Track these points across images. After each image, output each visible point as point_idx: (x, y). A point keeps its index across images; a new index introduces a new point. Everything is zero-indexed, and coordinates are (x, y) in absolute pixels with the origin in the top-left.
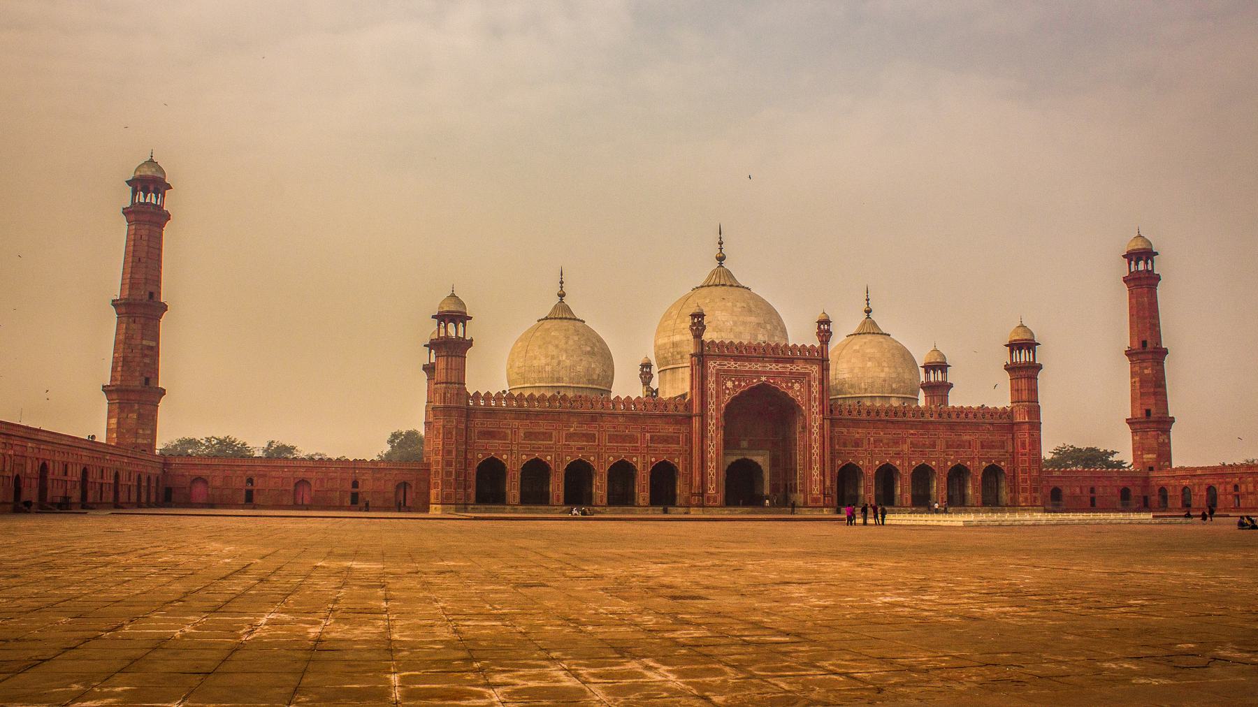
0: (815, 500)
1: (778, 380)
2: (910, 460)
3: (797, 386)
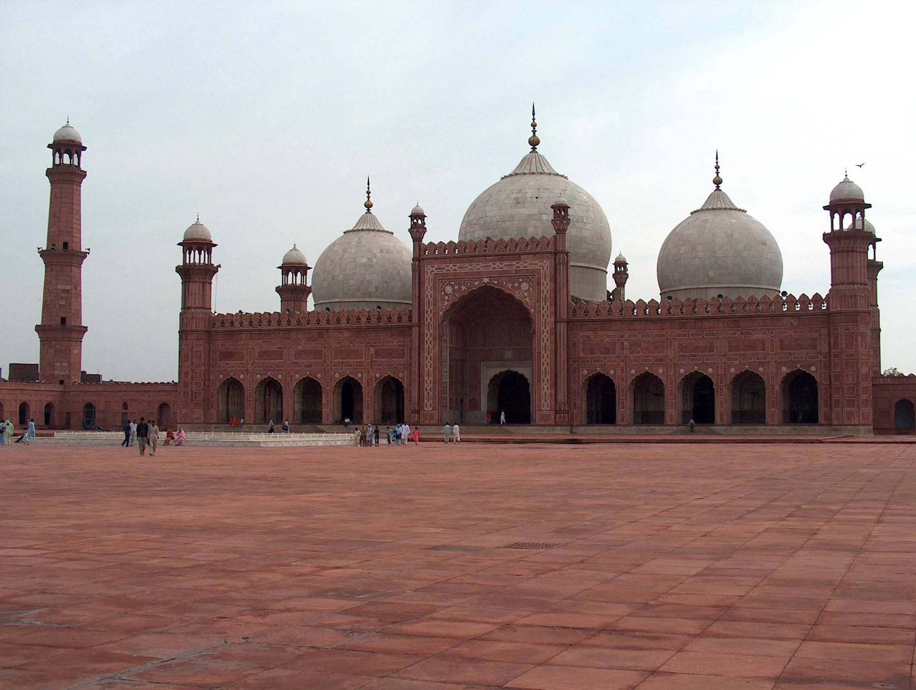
3: (525, 286)
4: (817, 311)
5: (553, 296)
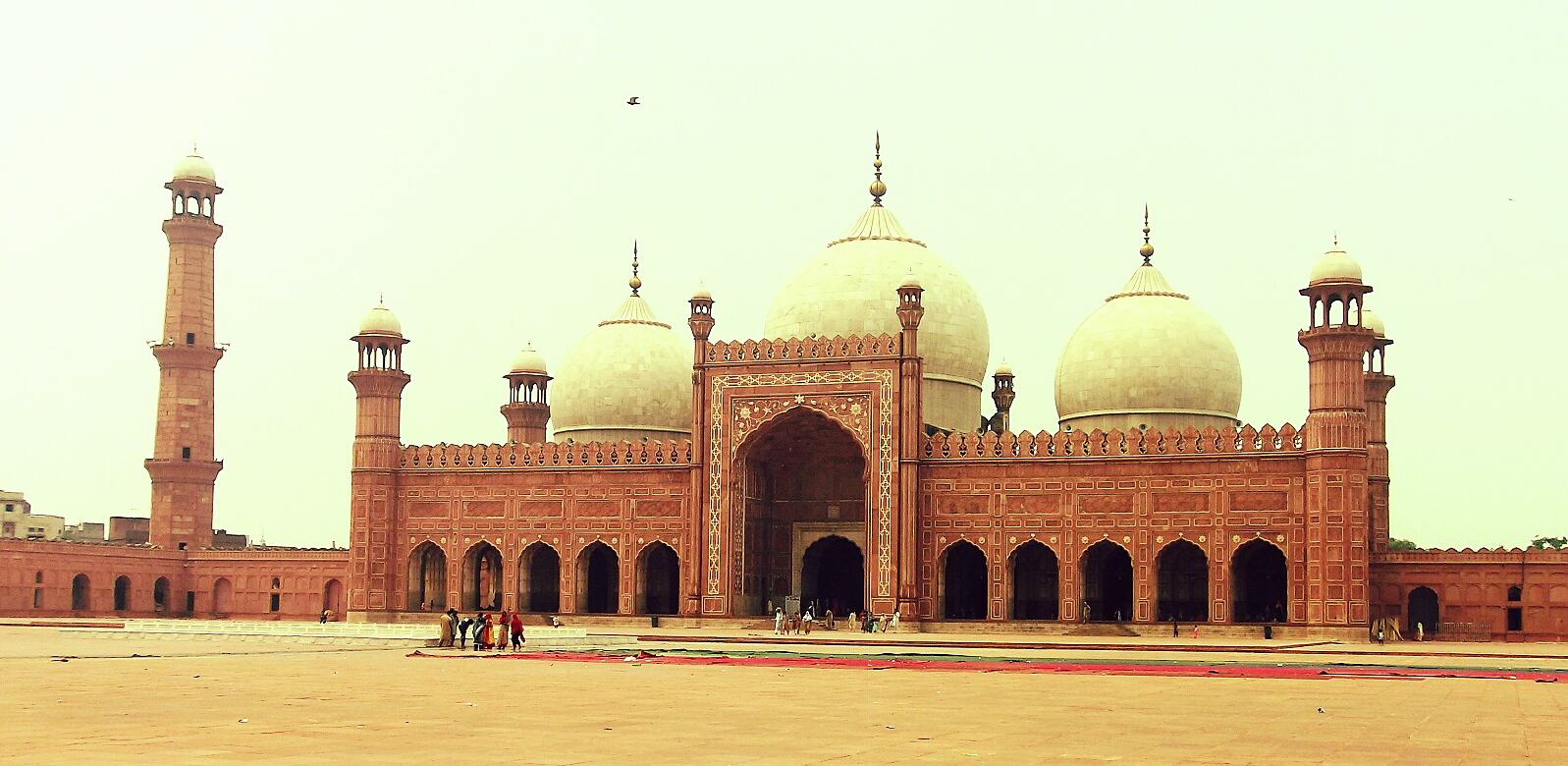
0: (883, 608)
1: (824, 398)
2: (1079, 533)
3: (856, 408)
4: (1287, 451)
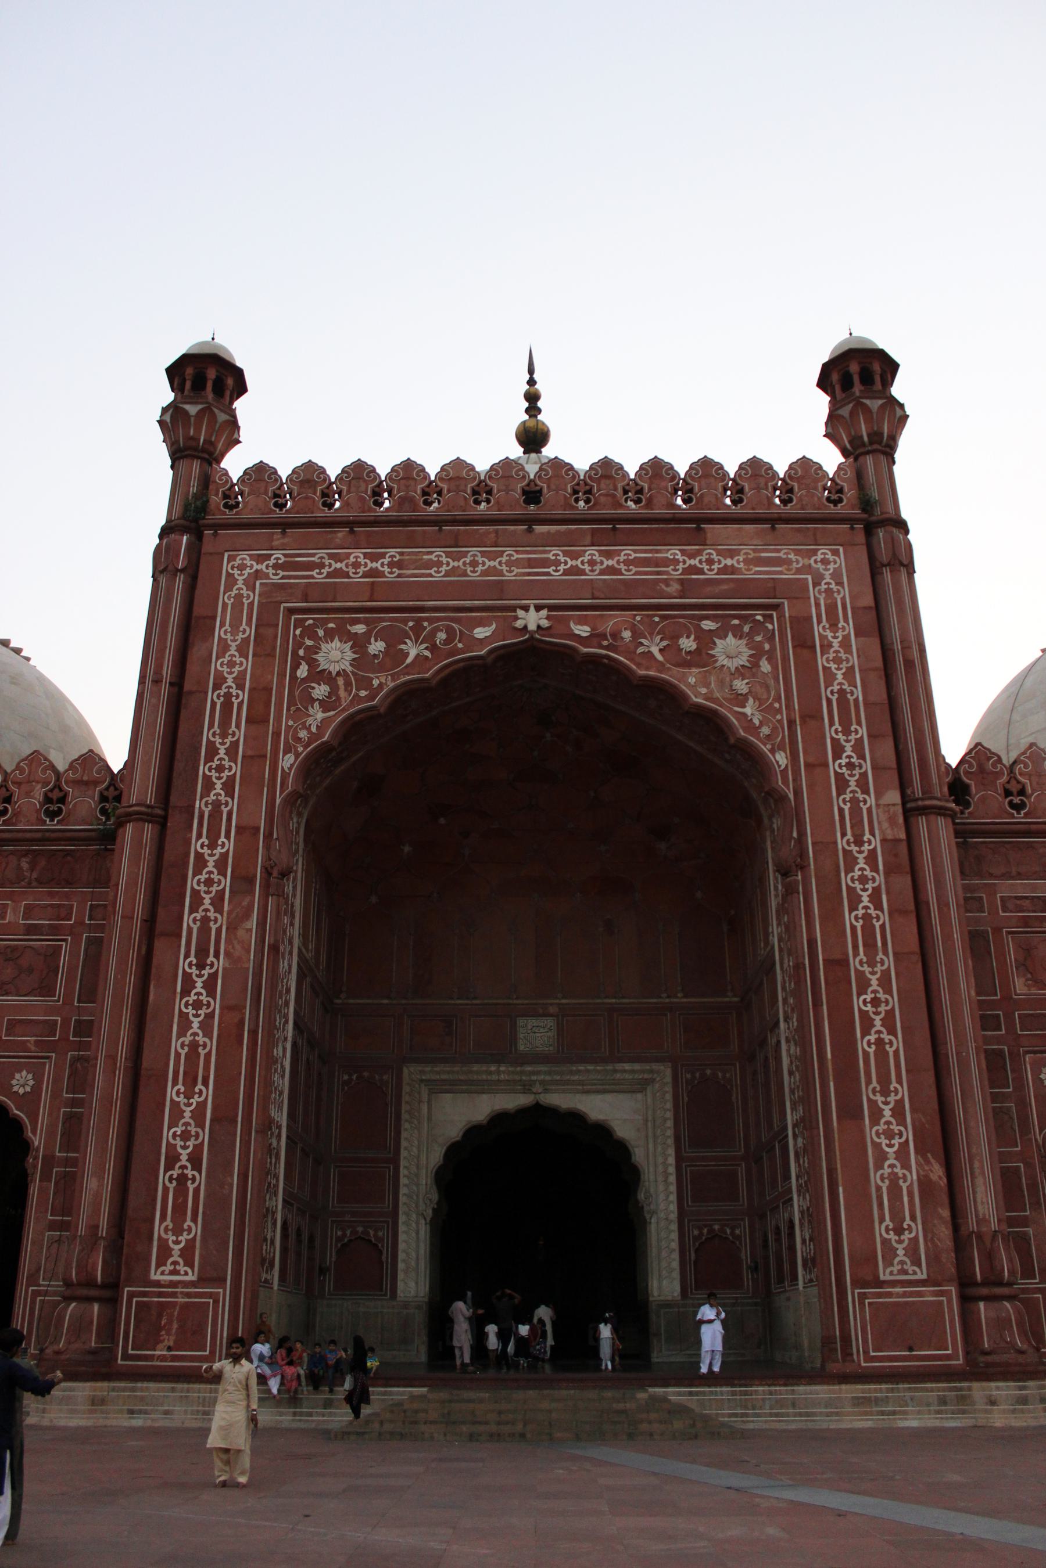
0: (898, 1325)
1: (612, 621)
3: (731, 651)
5: (880, 694)
